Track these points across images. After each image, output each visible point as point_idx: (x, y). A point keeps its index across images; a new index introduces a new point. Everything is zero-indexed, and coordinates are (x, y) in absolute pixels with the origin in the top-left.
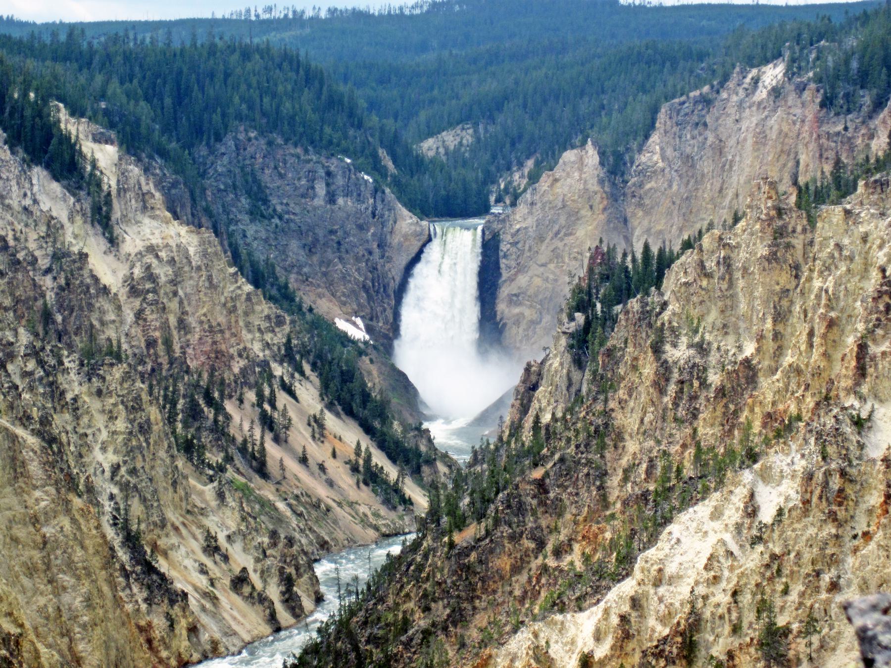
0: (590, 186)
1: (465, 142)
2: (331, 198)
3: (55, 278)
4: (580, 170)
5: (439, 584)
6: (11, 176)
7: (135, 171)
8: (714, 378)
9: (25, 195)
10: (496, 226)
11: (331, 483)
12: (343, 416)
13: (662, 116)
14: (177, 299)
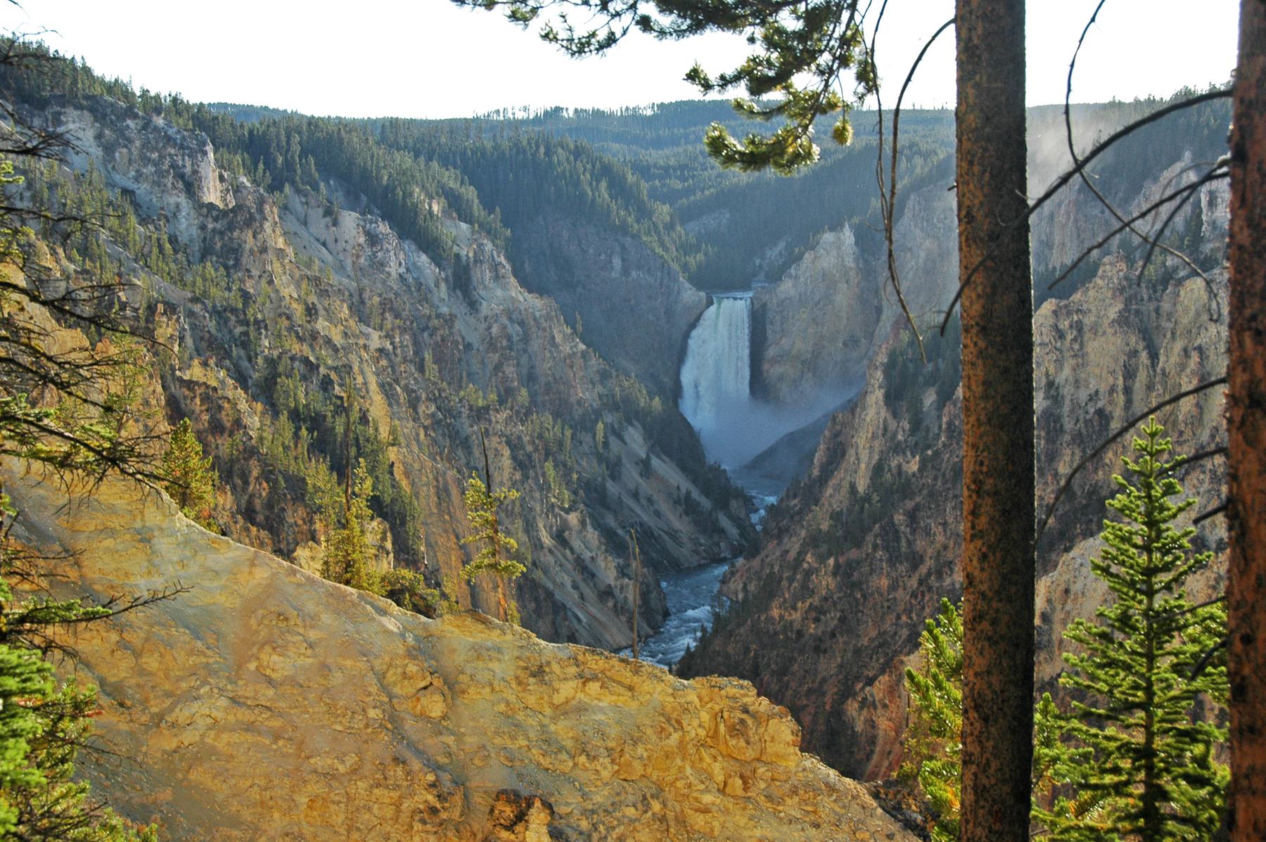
2: (626, 271)
3: (431, 335)
5: (826, 599)
6: (390, 248)
7: (489, 246)
8: (1068, 424)
9: (400, 264)
10: (766, 298)
11: (658, 514)
12: (664, 457)
14: (526, 355)
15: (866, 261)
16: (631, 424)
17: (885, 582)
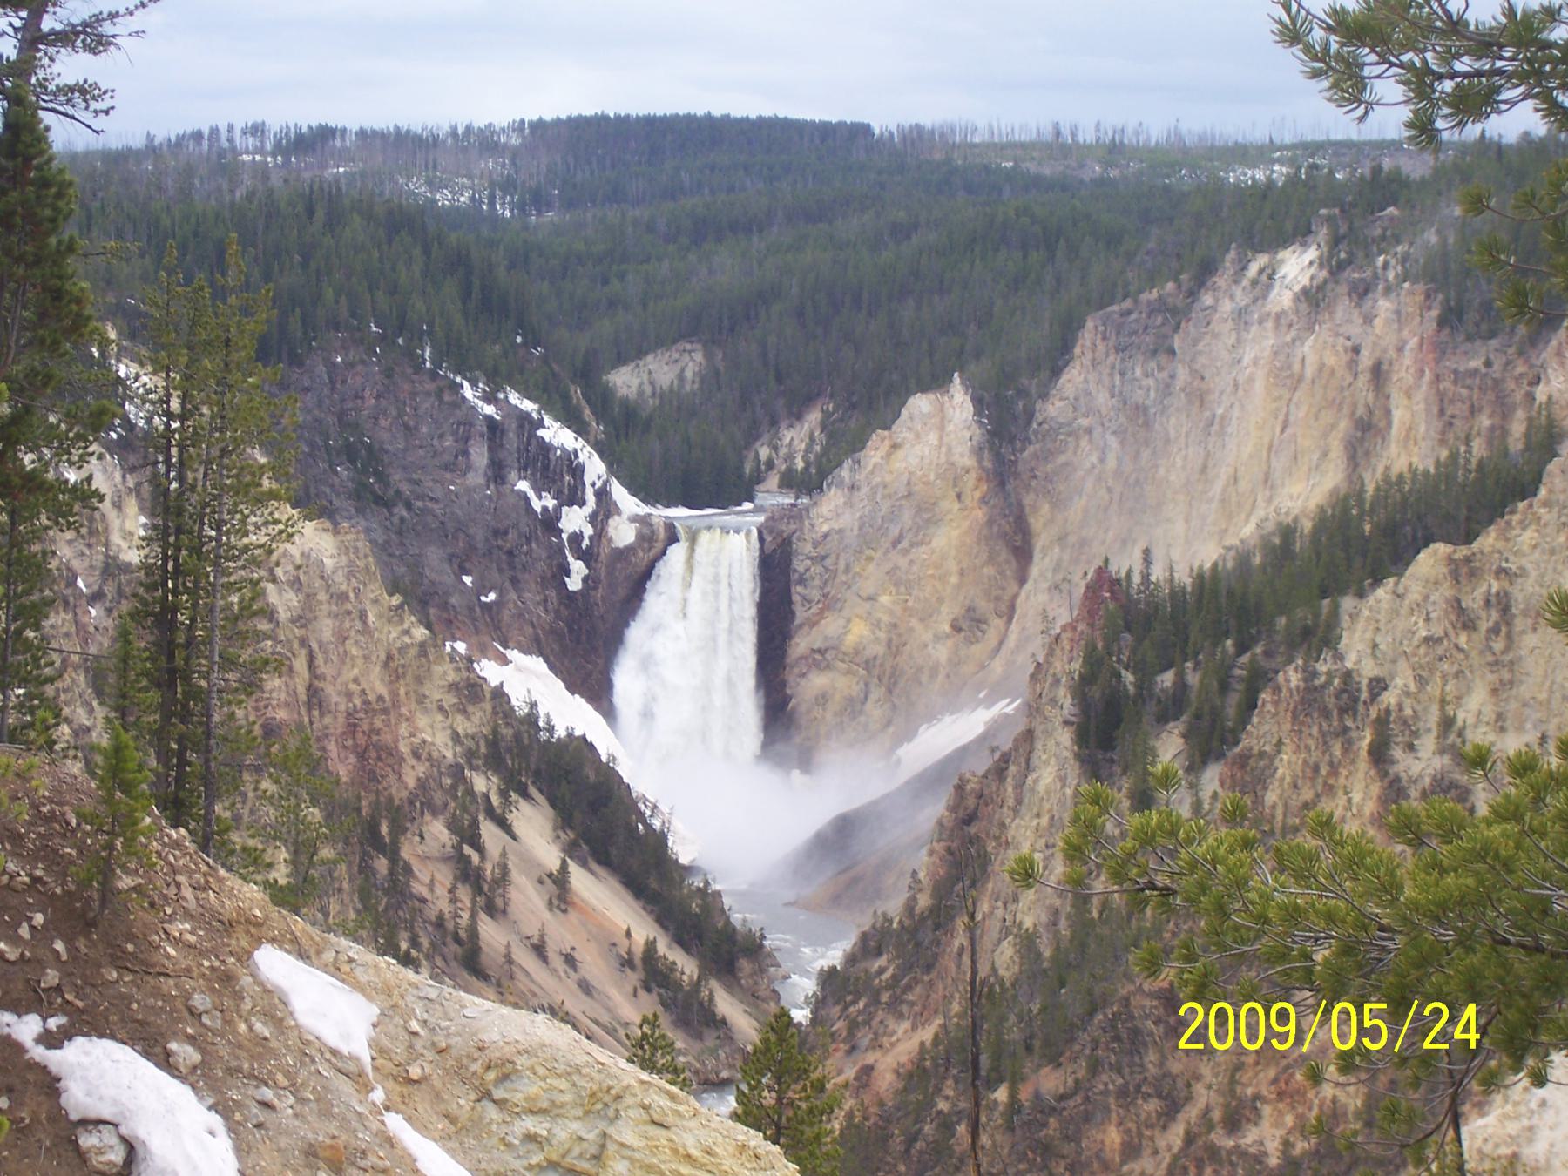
0: (956, 458)
1: (689, 374)
2: (497, 473)
4: (941, 428)
11: (586, 988)
13: (1088, 335)
15: (999, 458)
16: (525, 795)
17: (1113, 1137)
